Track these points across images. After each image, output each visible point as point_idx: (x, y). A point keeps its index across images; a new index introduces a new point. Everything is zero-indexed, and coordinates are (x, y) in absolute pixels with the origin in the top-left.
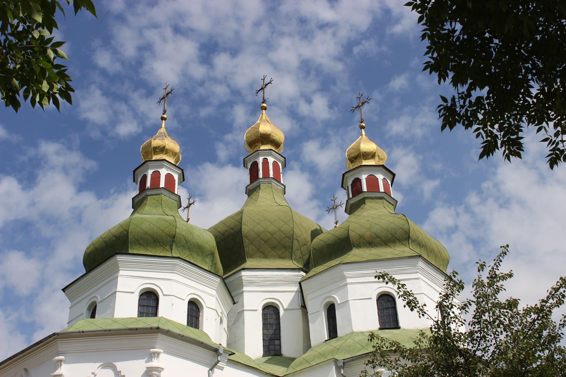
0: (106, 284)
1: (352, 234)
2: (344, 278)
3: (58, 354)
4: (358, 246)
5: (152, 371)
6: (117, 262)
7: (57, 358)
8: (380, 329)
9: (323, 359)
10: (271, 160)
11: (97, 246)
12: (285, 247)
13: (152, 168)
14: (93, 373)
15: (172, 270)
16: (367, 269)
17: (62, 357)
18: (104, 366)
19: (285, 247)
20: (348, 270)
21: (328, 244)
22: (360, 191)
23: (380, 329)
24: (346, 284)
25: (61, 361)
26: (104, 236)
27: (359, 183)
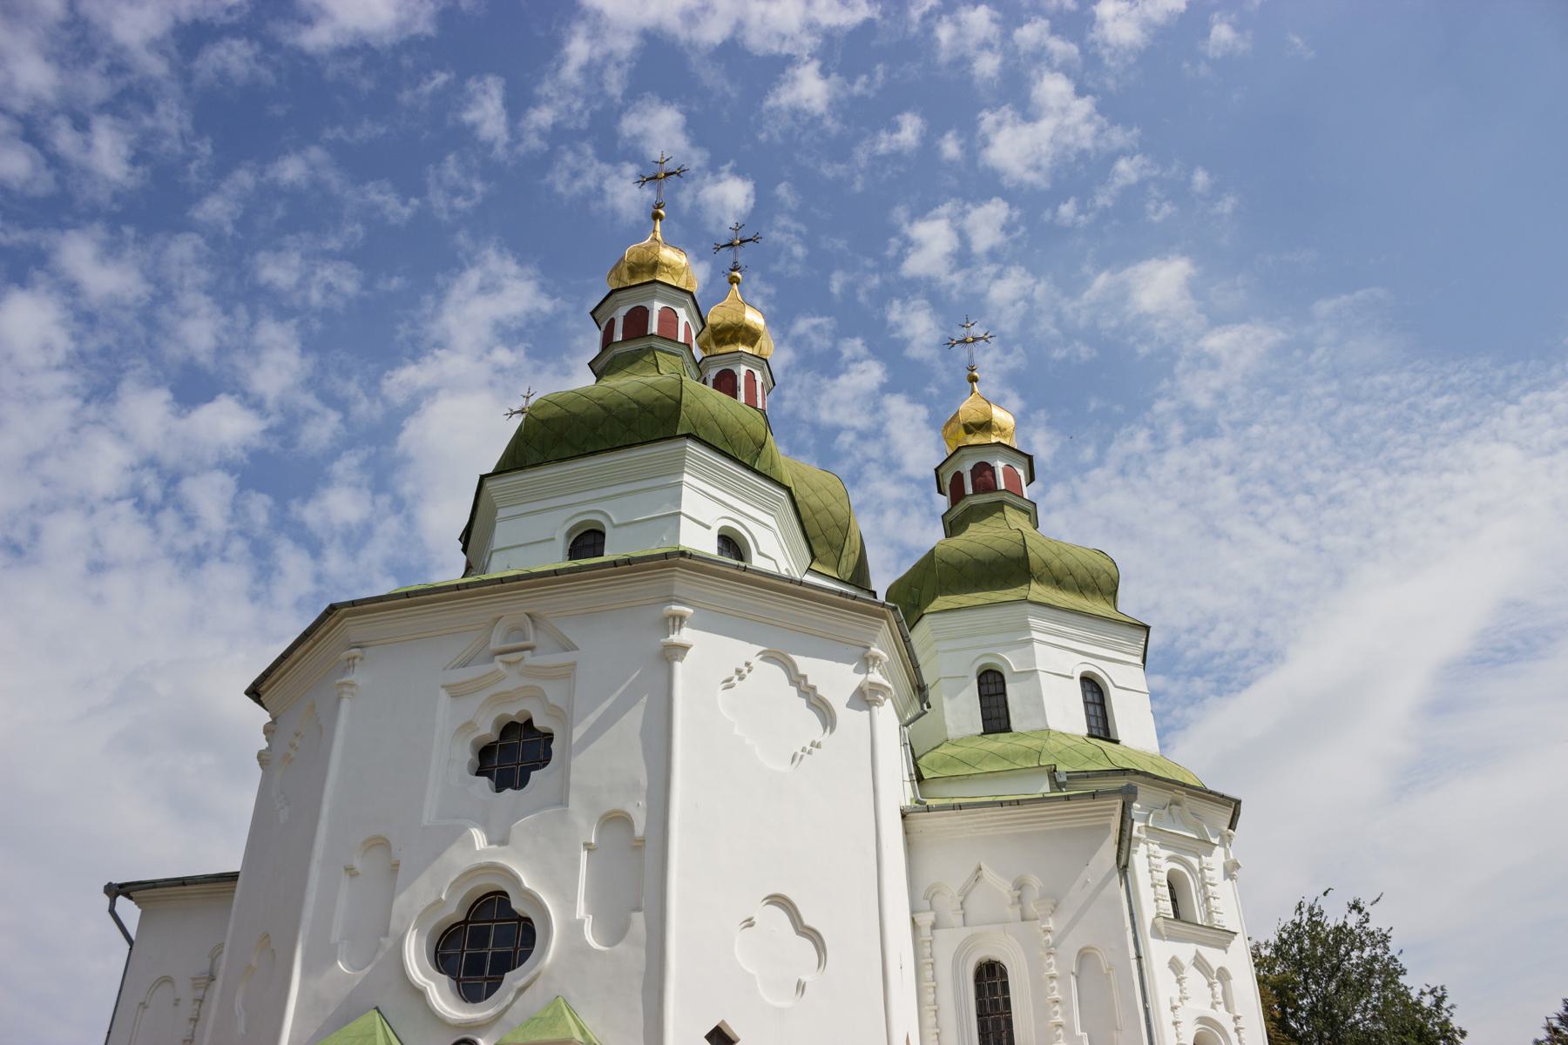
0: (627, 493)
1: (1031, 555)
2: (1027, 628)
3: (671, 601)
4: (1039, 580)
5: (877, 692)
6: (684, 452)
7: (676, 608)
8: (1091, 735)
9: (1006, 765)
10: (758, 375)
11: (573, 409)
12: (830, 544)
13: (662, 300)
14: (747, 664)
15: (770, 510)
16: (1066, 624)
17: (689, 611)
18: (767, 657)
19: (830, 544)
20: (1036, 617)
21: (977, 561)
22: (991, 487)
23: (1091, 735)
24: (1031, 641)
25: (682, 618)
26: (595, 395)
27: (988, 473)
